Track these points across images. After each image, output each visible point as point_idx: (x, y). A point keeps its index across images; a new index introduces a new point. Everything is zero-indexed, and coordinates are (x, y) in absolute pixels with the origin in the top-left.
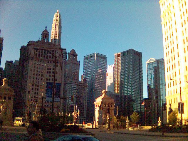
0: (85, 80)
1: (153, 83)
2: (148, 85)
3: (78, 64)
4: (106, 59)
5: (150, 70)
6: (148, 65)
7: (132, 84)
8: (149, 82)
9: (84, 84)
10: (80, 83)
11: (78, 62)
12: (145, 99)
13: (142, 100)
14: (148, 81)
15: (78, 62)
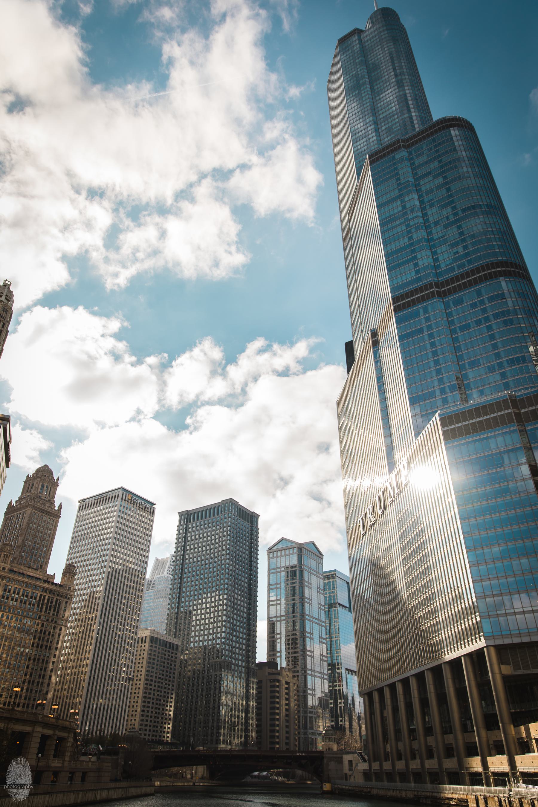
0: (70, 571)
1: (283, 614)
2: (269, 618)
3: (56, 515)
4: (152, 512)
5: (277, 572)
6: (273, 557)
7: (225, 602)
8: (273, 609)
9: (60, 586)
10: (49, 579)
11: (56, 508)
12: (261, 664)
13: (251, 669)
14: (269, 606)
15: (56, 508)
